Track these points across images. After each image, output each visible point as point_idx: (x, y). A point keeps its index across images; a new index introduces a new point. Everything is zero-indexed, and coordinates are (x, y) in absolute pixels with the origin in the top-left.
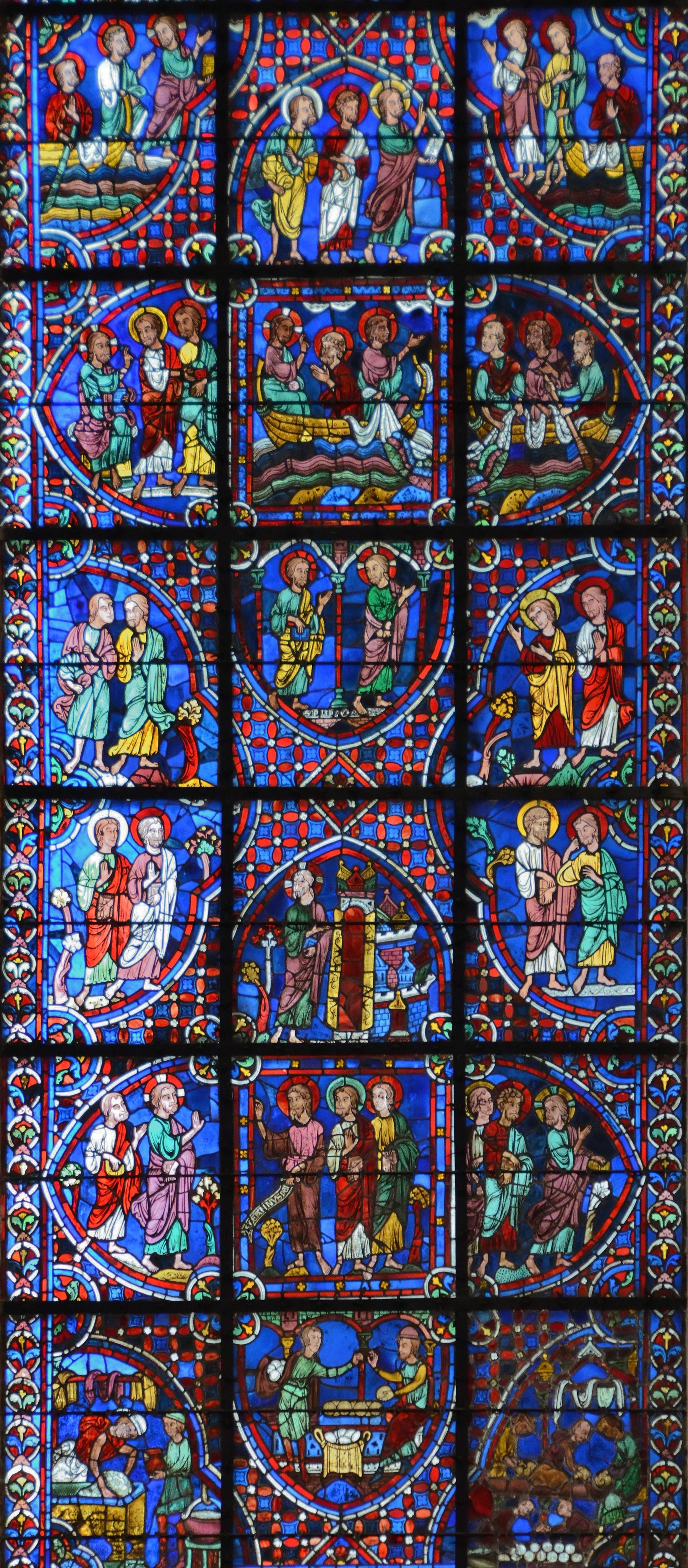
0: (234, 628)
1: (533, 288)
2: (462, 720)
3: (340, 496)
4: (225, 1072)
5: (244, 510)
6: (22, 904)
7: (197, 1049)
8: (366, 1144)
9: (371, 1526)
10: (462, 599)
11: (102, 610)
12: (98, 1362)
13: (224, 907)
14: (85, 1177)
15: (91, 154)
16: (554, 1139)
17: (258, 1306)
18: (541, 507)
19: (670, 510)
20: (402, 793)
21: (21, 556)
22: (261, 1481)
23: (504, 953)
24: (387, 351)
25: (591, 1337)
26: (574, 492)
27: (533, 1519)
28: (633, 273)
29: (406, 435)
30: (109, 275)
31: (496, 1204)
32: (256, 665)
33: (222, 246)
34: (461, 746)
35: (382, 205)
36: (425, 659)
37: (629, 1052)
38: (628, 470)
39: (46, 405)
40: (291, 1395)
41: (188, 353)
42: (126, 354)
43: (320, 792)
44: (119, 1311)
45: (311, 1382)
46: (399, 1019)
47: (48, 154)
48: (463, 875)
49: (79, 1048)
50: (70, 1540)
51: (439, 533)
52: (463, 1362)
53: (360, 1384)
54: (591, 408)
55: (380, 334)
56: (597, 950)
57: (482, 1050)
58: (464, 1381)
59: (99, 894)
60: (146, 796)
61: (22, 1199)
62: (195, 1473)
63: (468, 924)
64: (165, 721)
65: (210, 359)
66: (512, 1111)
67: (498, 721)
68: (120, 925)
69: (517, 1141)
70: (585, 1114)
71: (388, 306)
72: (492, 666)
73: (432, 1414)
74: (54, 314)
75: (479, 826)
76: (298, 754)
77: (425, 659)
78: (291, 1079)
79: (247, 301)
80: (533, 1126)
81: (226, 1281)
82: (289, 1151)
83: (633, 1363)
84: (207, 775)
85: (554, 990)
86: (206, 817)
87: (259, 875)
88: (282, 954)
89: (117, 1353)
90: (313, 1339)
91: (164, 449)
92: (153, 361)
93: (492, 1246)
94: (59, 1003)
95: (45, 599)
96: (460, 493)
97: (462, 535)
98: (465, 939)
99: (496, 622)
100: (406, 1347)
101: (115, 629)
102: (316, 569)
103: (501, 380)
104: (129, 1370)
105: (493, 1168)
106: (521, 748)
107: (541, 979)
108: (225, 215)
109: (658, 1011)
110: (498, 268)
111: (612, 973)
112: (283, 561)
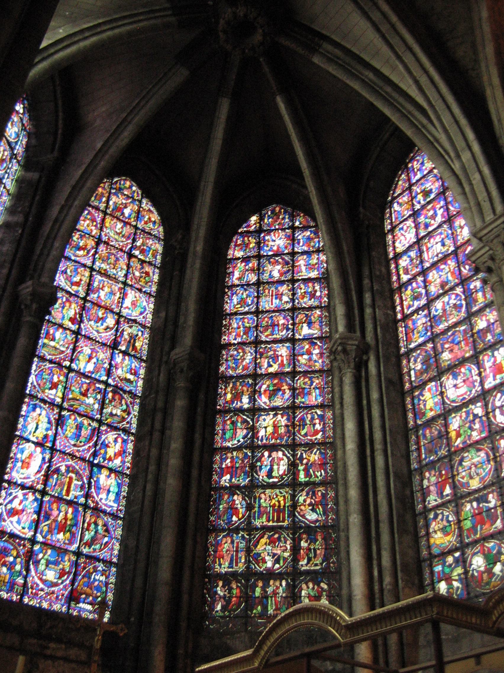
0: (60, 422)
8: (66, 518)
9: (53, 593)
12: (6, 544)
15: (52, 343)
18: (113, 423)
25: (101, 567)
27: (85, 599)
29: (94, 404)
30: (51, 362)
34: (95, 455)
35: (97, 369)
38: (128, 423)
39: (36, 376)
40: (43, 562)
42: (51, 374)
43: (69, 454)
46: (76, 497)
47: (46, 341)
52: (76, 564)
55: (93, 388)
62: (20, 572)
64: (45, 433)
65: (65, 380)
66: (93, 520)
67: (100, 454)
69: (93, 526)
70: (105, 525)
73: (69, 573)
74: (41, 364)
75: (95, 469)
76: (66, 446)
77: (91, 439)
81: (34, 536)
83: (107, 573)
87: (56, 464)
97: (100, 422)
101: (40, 415)
102: (75, 419)
104: (12, 547)
105: (88, 529)
109: (121, 511)
112: (70, 415)
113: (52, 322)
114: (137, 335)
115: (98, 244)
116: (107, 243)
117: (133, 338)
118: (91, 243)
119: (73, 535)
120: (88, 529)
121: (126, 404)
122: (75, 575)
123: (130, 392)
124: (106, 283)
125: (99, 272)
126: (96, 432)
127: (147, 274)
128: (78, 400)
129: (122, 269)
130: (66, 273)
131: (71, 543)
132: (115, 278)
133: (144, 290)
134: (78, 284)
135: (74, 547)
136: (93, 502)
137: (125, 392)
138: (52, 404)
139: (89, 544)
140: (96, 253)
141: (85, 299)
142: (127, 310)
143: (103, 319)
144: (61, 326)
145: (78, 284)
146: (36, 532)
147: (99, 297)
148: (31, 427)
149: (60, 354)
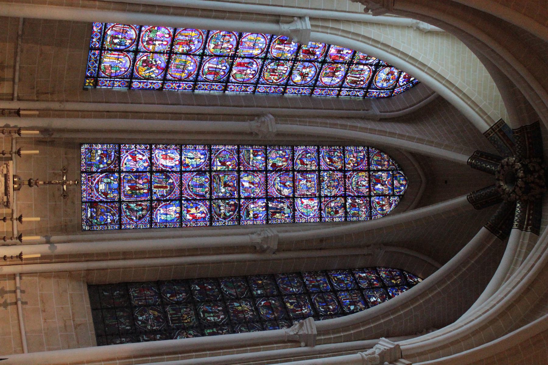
0: (200, 172)
1: (238, 207)
2: (190, 200)
3: (215, 185)
4: (149, 172)
5: (213, 174)
6: (168, 147)
7: (151, 168)
8: (140, 189)
9: (92, 191)
10: (203, 200)
11: (202, 157)
12: (113, 156)
13: (168, 171)
14: (136, 155)
15: (252, 156)
16: (141, 212)
17: (120, 176)
19: (213, 224)
20: (181, 193)
21: (208, 147)
22: (98, 176)
23: (163, 206)
24: (231, 190)
25: (116, 218)
26: (215, 213)
27: (93, 211)
28: (239, 219)
30: (239, 158)
31: (133, 205)
32: (196, 175)
33: (242, 171)
34: (187, 200)
35: (246, 189)
36: (197, 195)
37: (151, 222)
39: (225, 150)
40: (109, 180)
41: (230, 167)
42: (230, 160)
43: (181, 183)
44: (119, 159)
45: (111, 183)
46: (155, 193)
47: (251, 151)
48: (172, 200)
49: (151, 154)
50: (91, 152)
51: (211, 197)
52: (113, 202)
53: (110, 189)
54: (225, 214)
55: (233, 189)
56: (163, 217)
57: (151, 203)
58: (111, 202)
59: (169, 156)
60: (181, 162)
61: (133, 146)
62: (99, 168)
63: (166, 201)
64: (190, 164)
66: (144, 207)
68: (166, 159)
69: (140, 208)
70: (144, 216)
71: (236, 190)
72: (196, 203)
73: (107, 198)
75: (178, 202)
77: (197, 195)
78: (148, 180)
79: (236, 174)
80: (142, 210)
81: (123, 172)
82: (139, 180)
83: (113, 223)
84: (183, 169)
85: (159, 212)
86: (179, 169)
88: (163, 178)
89: (114, 158)
90: (116, 183)
91: (220, 164)
92: (229, 163)
93: (127, 205)
94: (157, 151)
95: (203, 150)
96: (215, 199)
97: (210, 199)
98: (164, 201)
99: (201, 204)
100: (115, 195)
101: (200, 158)
102: (207, 182)
103: (228, 204)
105: (137, 205)
106: (187, 207)
107: (160, 210)
108: (246, 171)
109: (156, 225)
110: (240, 203)
111: (160, 219)
113: (266, 152)
114: (285, 214)
115: (340, 170)
116: (345, 177)
117: (281, 211)
118: (339, 165)
119: (131, 196)
120: (137, 205)
121: (230, 216)
122: (107, 202)
123: (240, 217)
124: (313, 183)
125: (319, 177)
126: (203, 198)
127: (337, 212)
128: (220, 181)
129: (330, 192)
130: (307, 154)
131: (125, 196)
132: (320, 189)
133: (322, 212)
134: (303, 163)
135: (123, 198)
136: (156, 205)
137: (239, 212)
138: (211, 165)
139: (128, 207)
140: (334, 171)
141: (294, 170)
142: (300, 202)
143: (285, 186)
144: (266, 159)
145: (303, 163)
146: (125, 172)
147: (300, 180)
148: (190, 155)
149: (247, 162)
